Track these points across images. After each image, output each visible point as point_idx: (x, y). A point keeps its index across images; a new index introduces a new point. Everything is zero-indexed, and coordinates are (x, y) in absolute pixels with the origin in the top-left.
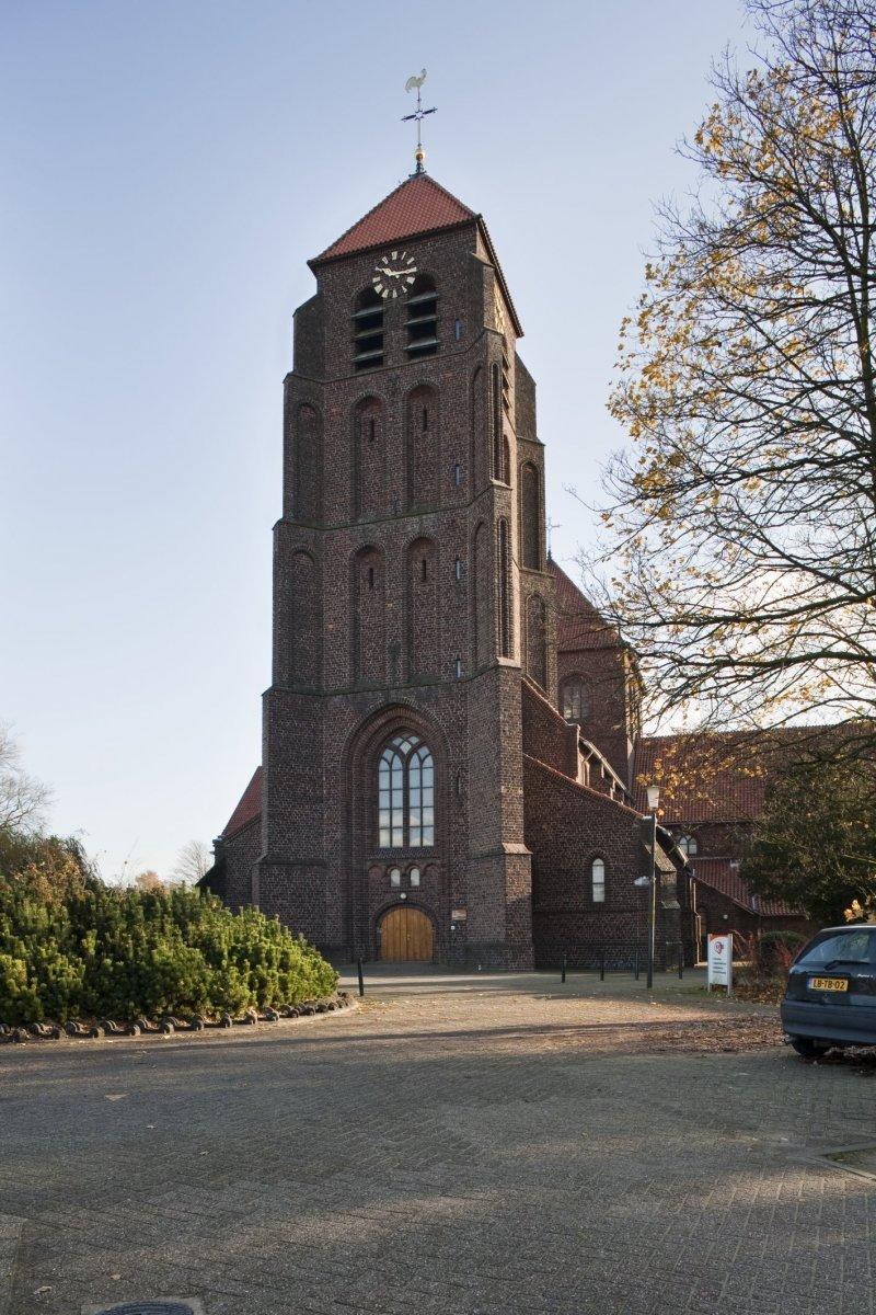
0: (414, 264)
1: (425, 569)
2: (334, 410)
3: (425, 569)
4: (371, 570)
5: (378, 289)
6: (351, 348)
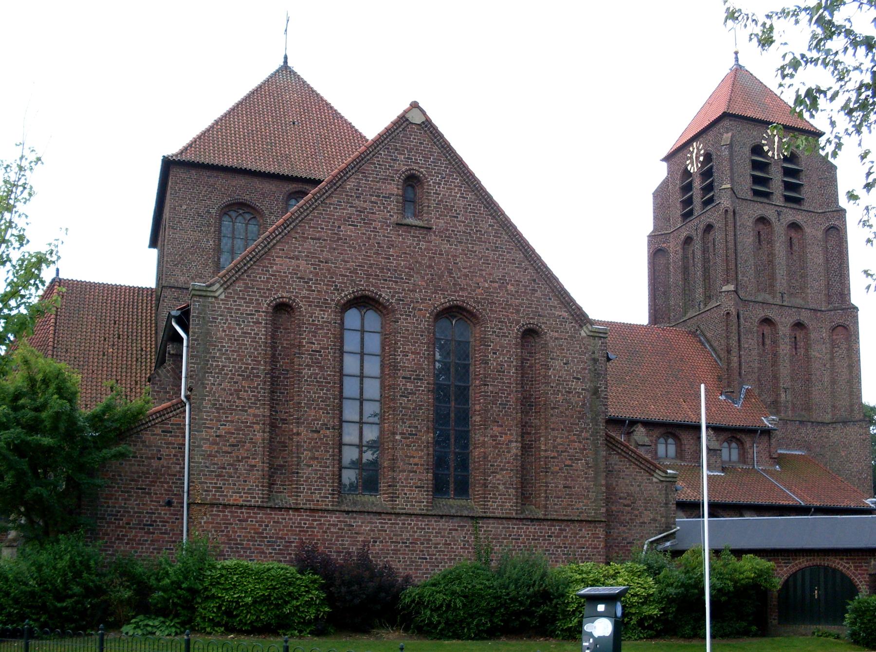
5: (766, 148)
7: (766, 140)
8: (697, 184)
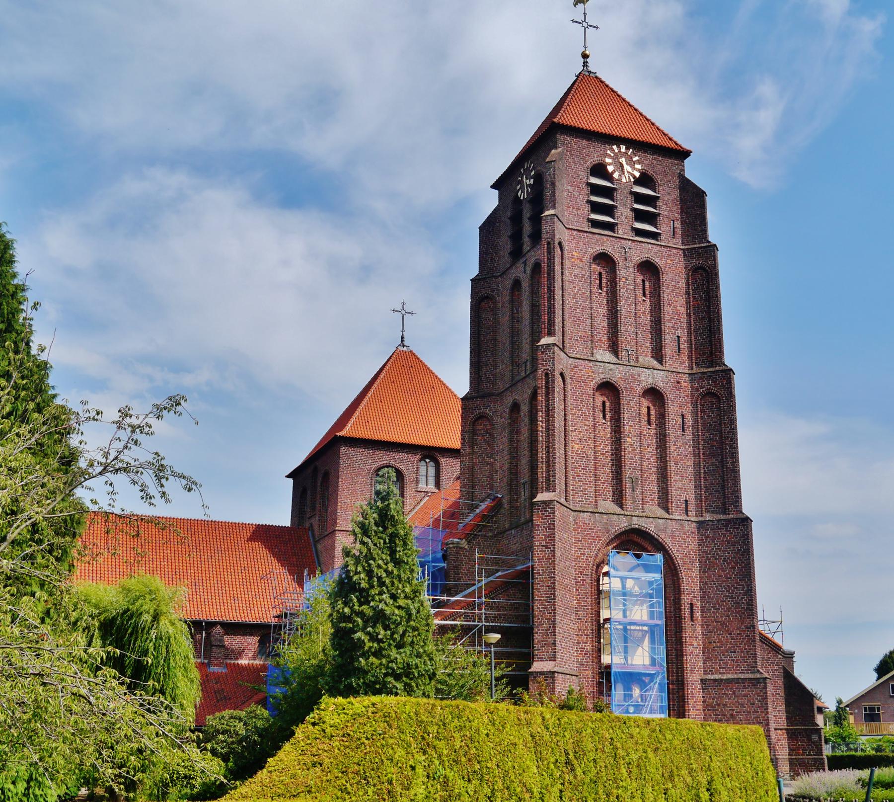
0: (639, 162)
2: (574, 253)
5: (610, 169)
6: (587, 208)
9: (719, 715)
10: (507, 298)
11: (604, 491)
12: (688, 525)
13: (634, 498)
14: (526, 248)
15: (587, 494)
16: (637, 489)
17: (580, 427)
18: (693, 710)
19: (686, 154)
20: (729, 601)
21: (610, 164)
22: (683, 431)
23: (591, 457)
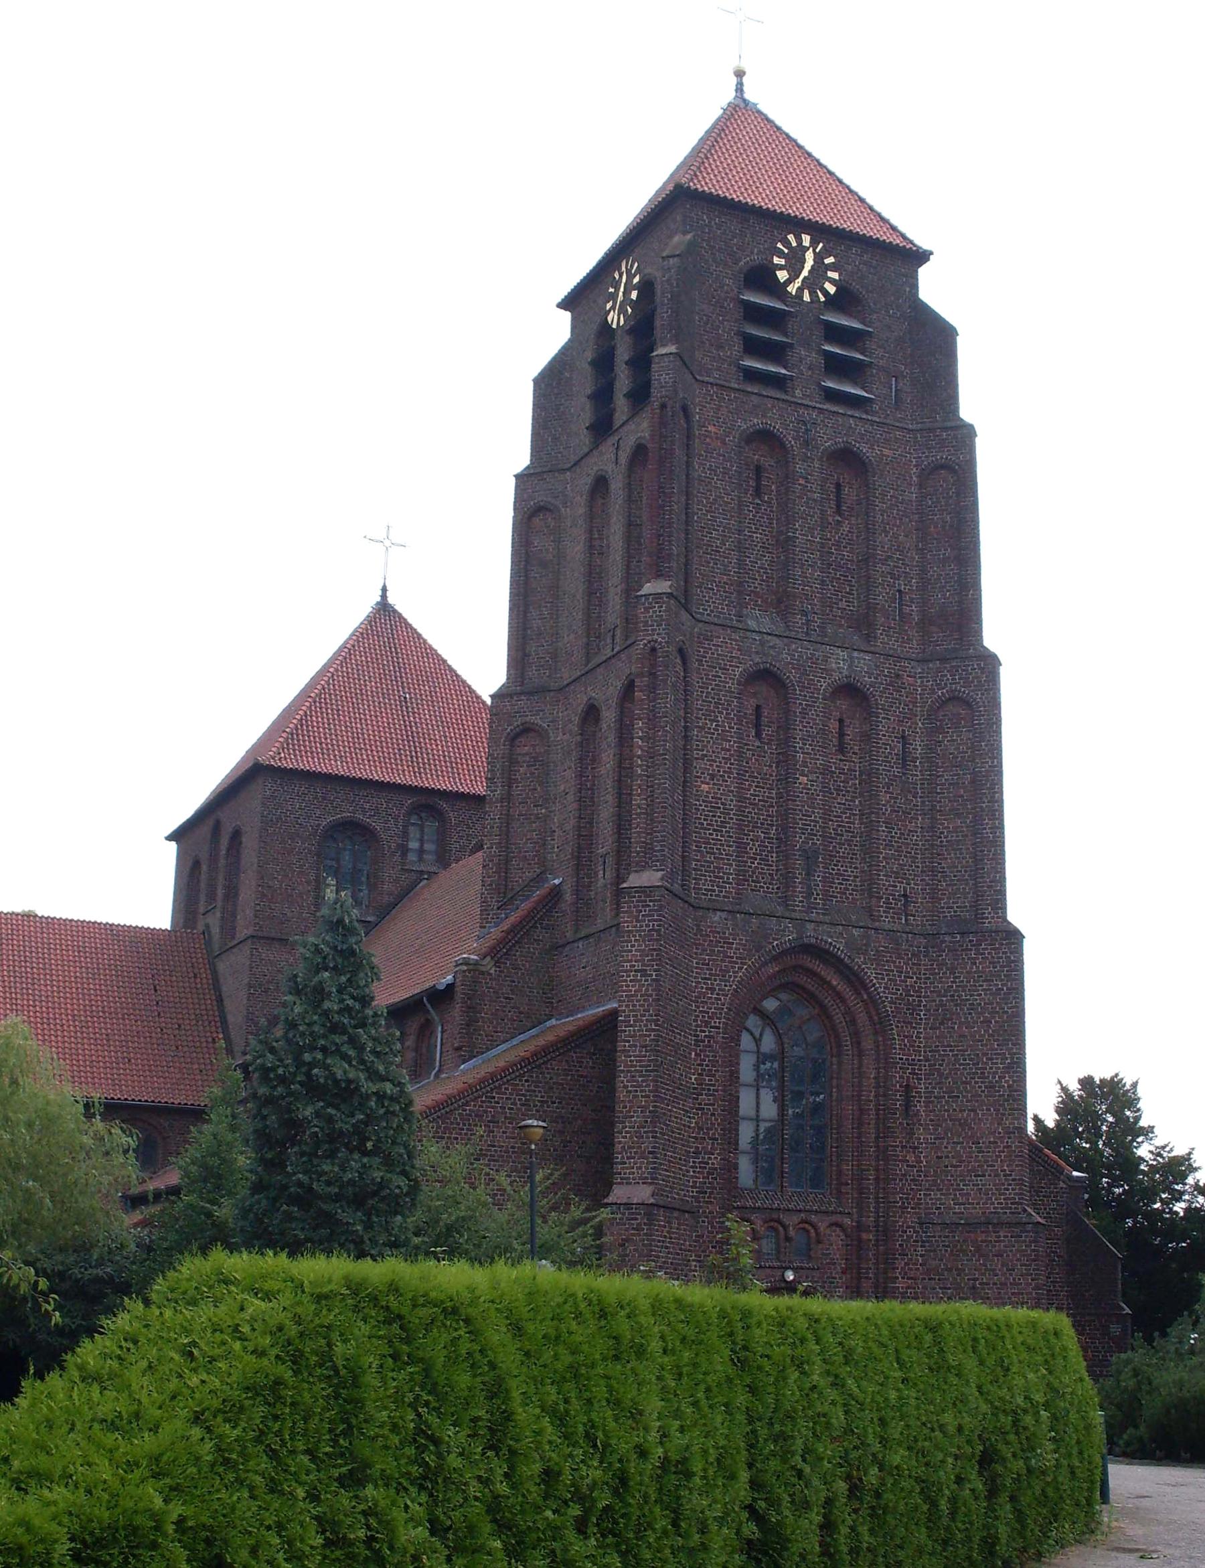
1: (841, 734)
3: (841, 734)
4: (758, 707)
5: (782, 275)
6: (737, 346)
7: (780, 254)
8: (623, 353)
9: (949, 1289)
10: (581, 511)
11: (754, 872)
12: (907, 941)
13: (809, 887)
14: (620, 416)
15: (723, 878)
16: (815, 871)
17: (713, 752)
18: (903, 1278)
19: (922, 257)
20: (976, 1083)
21: (781, 268)
22: (904, 766)
23: (732, 810)
